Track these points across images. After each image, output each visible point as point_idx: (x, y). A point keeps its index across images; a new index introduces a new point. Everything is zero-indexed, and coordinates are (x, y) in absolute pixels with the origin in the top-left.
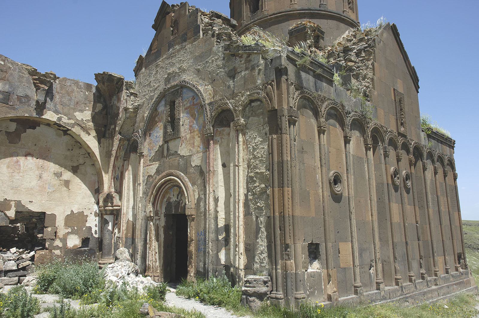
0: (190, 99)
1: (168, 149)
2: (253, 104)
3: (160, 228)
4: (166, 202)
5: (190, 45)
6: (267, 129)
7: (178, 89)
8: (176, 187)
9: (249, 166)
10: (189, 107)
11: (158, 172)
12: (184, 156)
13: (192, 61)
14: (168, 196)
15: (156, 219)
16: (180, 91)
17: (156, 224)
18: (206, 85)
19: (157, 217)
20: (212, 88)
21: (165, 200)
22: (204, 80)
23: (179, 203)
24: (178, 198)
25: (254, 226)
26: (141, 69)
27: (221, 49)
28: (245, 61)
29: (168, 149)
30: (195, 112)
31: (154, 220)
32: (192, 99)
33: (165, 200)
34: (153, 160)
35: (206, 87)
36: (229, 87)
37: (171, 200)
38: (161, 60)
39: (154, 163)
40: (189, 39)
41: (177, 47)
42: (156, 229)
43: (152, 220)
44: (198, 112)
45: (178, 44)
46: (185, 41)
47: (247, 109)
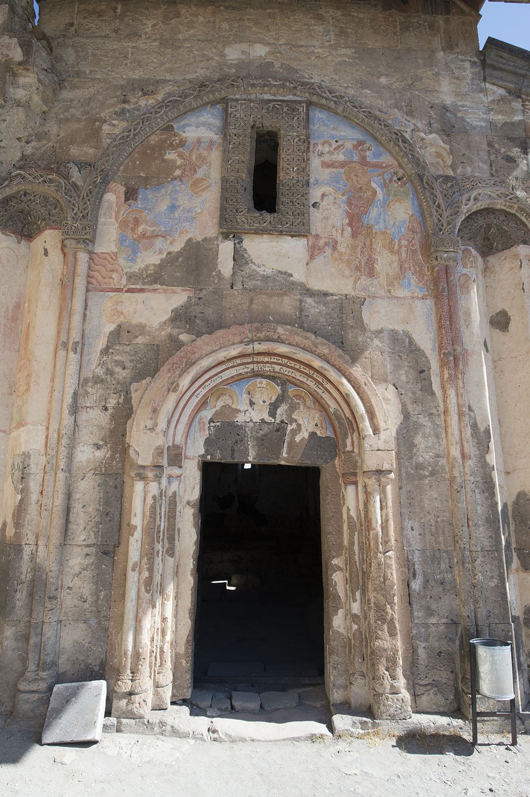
0: (349, 145)
1: (239, 258)
3: (179, 507)
4: (211, 421)
7: (300, 102)
8: (264, 381)
10: (343, 165)
12: (326, 294)
14: (220, 404)
15: (170, 477)
16: (302, 109)
17: (170, 493)
19: (175, 471)
21: (207, 414)
22: (410, 113)
23: (280, 429)
24: (272, 414)
29: (239, 258)
30: (373, 185)
31: (164, 481)
32: (355, 147)
33: (207, 414)
34: (157, 278)
35: (423, 135)
37: (240, 419)
39: (158, 286)
42: (167, 510)
43: (158, 478)
44: (384, 185)
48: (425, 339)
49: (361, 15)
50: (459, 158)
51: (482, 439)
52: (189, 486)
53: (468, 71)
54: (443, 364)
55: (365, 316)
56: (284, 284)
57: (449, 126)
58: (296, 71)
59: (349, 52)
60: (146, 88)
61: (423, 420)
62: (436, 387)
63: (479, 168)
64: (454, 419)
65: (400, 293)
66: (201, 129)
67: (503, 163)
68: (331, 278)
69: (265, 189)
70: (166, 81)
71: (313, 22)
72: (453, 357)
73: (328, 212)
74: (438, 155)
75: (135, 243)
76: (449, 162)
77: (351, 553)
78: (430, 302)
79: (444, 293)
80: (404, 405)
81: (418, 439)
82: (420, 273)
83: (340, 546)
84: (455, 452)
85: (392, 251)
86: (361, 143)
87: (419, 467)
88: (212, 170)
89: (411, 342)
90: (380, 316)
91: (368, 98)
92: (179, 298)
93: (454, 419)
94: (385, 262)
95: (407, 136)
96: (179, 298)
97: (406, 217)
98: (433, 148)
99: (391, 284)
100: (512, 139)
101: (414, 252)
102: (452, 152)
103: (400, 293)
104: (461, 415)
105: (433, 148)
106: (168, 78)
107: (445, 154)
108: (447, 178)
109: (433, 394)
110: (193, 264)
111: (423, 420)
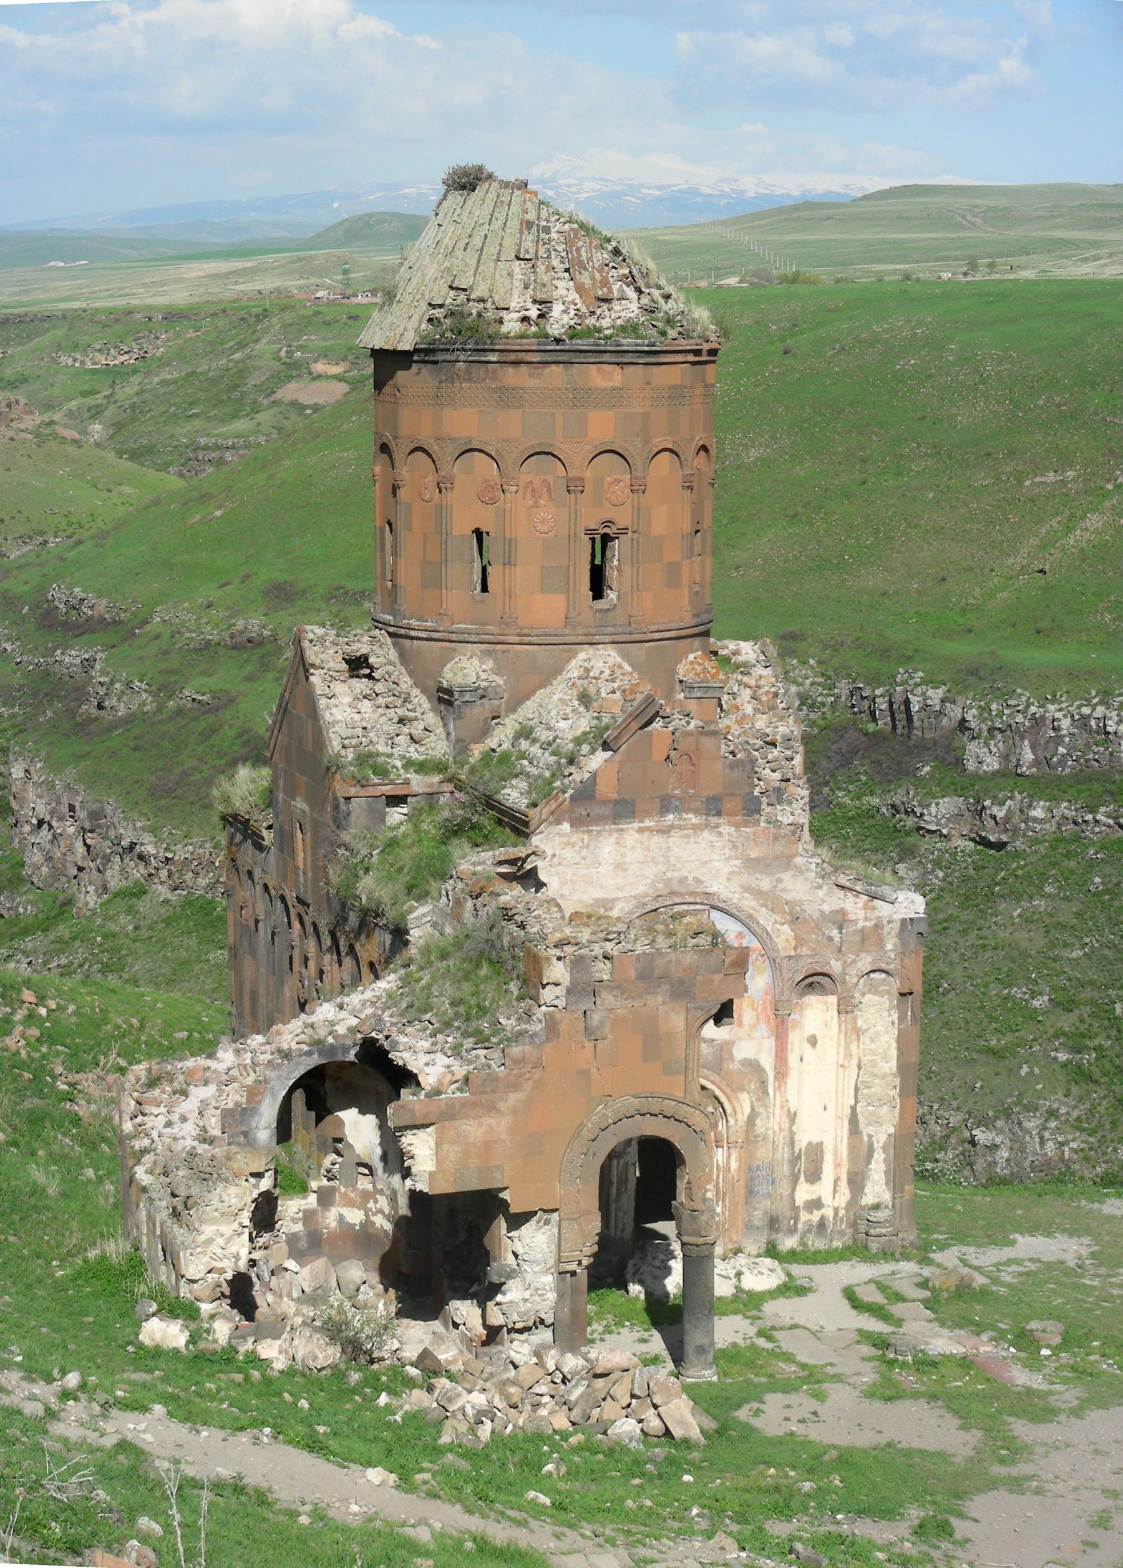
2: (872, 975)
5: (733, 829)
6: (895, 1017)
9: (859, 1067)
13: (738, 862)
18: (776, 922)
20: (792, 930)
22: (772, 910)
25: (865, 1148)
26: (558, 822)
27: (813, 866)
28: (865, 905)
32: (736, 937)
35: (778, 926)
36: (830, 939)
38: (636, 825)
40: (730, 814)
41: (693, 819)
45: (697, 812)
46: (719, 814)
47: (862, 980)
48: (767, 1062)
49: (748, 830)
51: (792, 1117)
54: (776, 1079)
55: (735, 1053)
58: (702, 882)
59: (738, 862)
61: (761, 1110)
62: (771, 1090)
64: (778, 1111)
65: (755, 1036)
67: (826, 942)
70: (619, 899)
71: (715, 839)
72: (781, 1073)
74: (787, 940)
76: (793, 943)
77: (718, 1183)
78: (773, 1040)
80: (752, 1103)
81: (758, 1122)
82: (768, 1022)
83: (711, 1179)
84: (777, 1128)
85: (753, 1009)
86: (740, 933)
87: (757, 1136)
89: (758, 1064)
93: (778, 1111)
95: (769, 929)
97: (763, 985)
99: (750, 1030)
100: (834, 923)
101: (766, 1008)
102: (796, 938)
103: (756, 1035)
104: (782, 1107)
106: (620, 895)
107: (791, 939)
108: (790, 957)
109: (768, 1094)
111: (761, 1110)
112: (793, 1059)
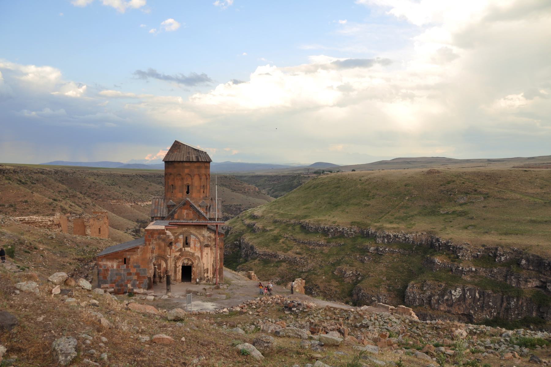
11: (180, 255)
34: (178, 251)
48: (200, 256)
50: (204, 240)
52: (181, 267)
53: (206, 230)
56: (188, 252)
57: (203, 236)
60: (176, 233)
63: (206, 241)
66: (181, 237)
68: (192, 251)
69: (187, 243)
73: (192, 245)
75: (176, 248)
79: (202, 252)
88: (182, 241)
90: (196, 254)
91: (196, 234)
92: (180, 253)
94: (197, 250)
96: (180, 253)
98: (202, 239)
105: (202, 239)
110: (180, 250)
112: (204, 256)
